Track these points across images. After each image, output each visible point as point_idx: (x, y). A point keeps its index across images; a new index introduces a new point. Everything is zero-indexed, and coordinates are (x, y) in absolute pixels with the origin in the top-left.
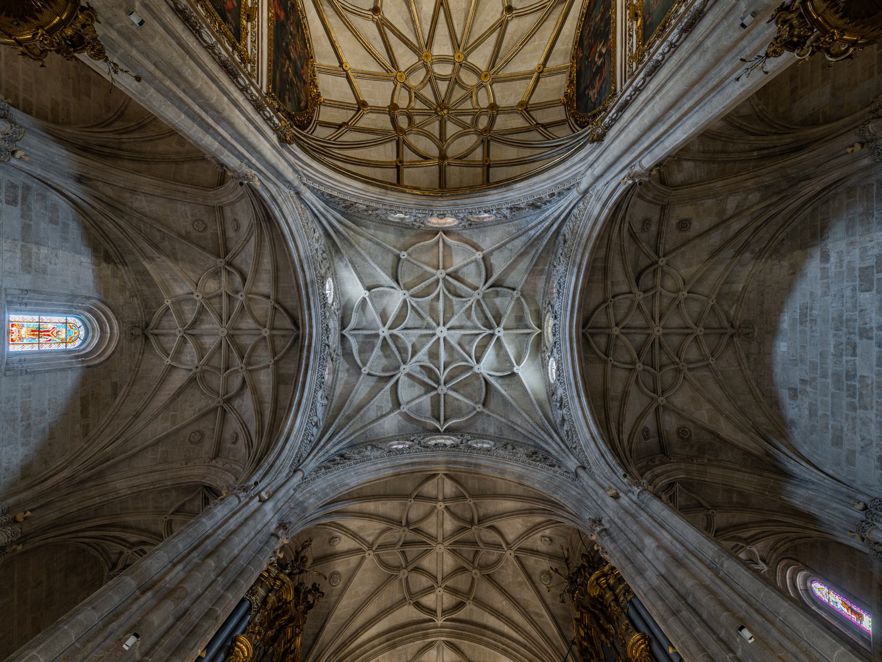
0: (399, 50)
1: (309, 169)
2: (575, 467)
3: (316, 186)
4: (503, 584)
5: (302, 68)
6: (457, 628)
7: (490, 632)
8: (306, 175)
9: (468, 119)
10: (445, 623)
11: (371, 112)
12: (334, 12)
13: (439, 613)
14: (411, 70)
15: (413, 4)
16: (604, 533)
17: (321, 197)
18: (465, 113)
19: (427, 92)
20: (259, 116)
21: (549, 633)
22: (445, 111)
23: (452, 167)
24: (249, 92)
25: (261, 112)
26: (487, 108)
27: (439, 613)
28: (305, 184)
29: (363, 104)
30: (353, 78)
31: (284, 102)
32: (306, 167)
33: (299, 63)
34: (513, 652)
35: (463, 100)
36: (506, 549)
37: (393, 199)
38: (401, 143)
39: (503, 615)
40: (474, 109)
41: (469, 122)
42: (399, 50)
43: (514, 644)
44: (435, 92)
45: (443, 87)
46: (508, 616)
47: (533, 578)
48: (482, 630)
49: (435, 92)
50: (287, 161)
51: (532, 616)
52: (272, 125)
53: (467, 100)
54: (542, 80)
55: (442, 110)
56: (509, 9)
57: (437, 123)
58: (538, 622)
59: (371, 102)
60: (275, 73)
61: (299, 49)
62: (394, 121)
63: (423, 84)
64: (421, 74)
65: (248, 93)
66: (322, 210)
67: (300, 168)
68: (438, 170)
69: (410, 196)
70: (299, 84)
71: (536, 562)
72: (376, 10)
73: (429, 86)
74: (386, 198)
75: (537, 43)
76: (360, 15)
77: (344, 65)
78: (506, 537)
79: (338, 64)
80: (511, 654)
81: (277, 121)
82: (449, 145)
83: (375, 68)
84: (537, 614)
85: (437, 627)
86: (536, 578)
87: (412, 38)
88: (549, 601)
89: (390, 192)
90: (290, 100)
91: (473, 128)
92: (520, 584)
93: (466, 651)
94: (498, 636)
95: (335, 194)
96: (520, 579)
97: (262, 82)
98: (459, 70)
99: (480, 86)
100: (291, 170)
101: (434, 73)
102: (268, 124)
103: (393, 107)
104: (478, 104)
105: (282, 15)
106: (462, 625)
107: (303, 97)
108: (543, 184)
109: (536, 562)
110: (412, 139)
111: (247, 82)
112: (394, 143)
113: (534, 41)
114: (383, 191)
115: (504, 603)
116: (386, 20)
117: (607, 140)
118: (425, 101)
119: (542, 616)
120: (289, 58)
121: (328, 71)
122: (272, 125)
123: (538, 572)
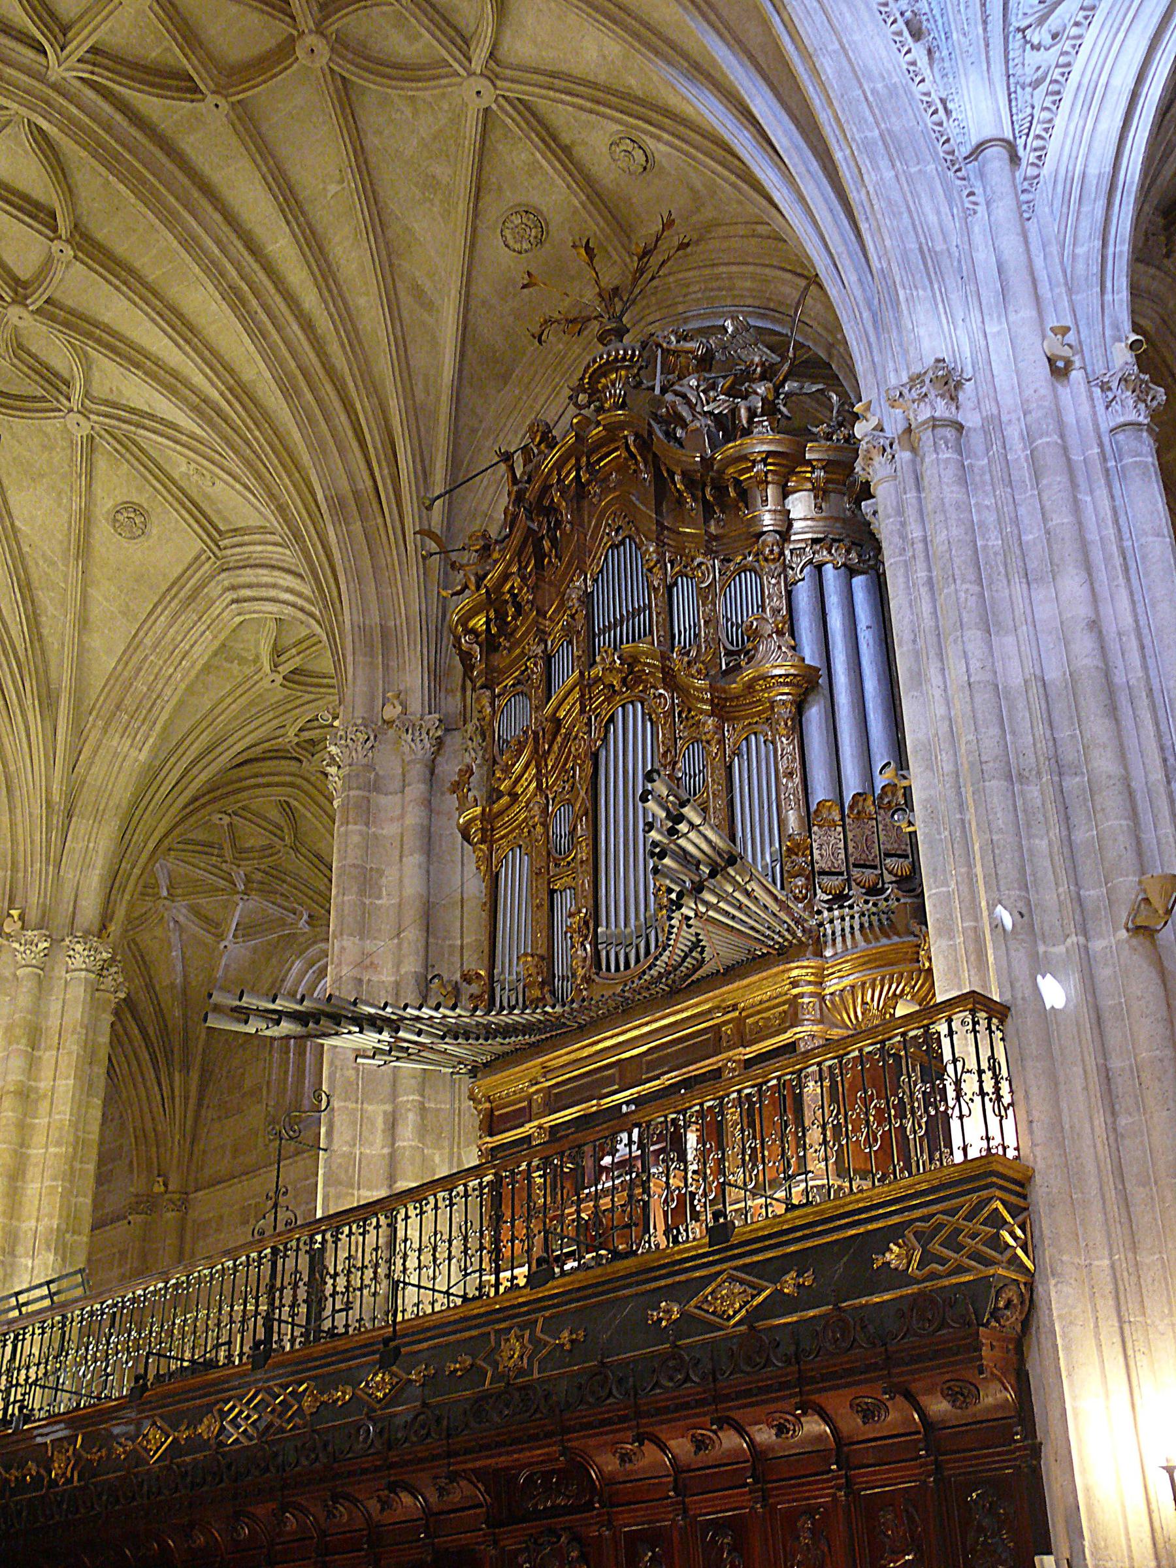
2: (989, 132)
4: (372, 141)
6: (108, 129)
7: (218, 217)
10: (77, 83)
13: (79, 46)
16: (950, 433)
21: (420, 359)
27: (79, 46)
34: (263, 317)
36: (477, 66)
39: (303, 213)
43: (278, 299)
46: (319, 229)
47: (487, 199)
48: (196, 194)
51: (399, 284)
58: (405, 314)
71: (533, 169)
78: (508, 34)
80: (253, 316)
84: (418, 292)
85: (41, 78)
86: (493, 209)
88: (482, 288)
92: (430, 184)
93: (83, 193)
94: (239, 245)
96: (441, 171)
106: (133, 131)
109: (533, 169)
115: (333, 188)
119: (429, 306)
123: (511, 198)
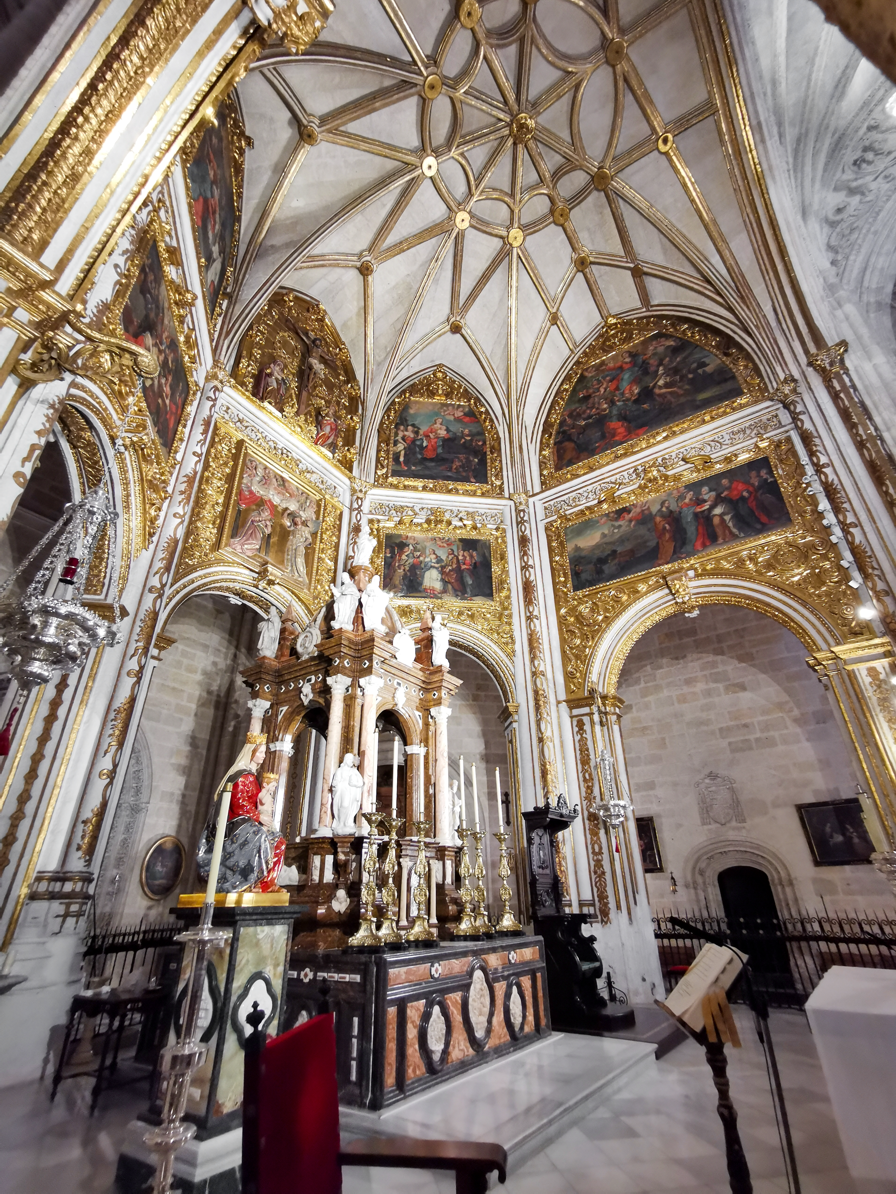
0: (473, 267)
42: (473, 267)
121: (565, 332)
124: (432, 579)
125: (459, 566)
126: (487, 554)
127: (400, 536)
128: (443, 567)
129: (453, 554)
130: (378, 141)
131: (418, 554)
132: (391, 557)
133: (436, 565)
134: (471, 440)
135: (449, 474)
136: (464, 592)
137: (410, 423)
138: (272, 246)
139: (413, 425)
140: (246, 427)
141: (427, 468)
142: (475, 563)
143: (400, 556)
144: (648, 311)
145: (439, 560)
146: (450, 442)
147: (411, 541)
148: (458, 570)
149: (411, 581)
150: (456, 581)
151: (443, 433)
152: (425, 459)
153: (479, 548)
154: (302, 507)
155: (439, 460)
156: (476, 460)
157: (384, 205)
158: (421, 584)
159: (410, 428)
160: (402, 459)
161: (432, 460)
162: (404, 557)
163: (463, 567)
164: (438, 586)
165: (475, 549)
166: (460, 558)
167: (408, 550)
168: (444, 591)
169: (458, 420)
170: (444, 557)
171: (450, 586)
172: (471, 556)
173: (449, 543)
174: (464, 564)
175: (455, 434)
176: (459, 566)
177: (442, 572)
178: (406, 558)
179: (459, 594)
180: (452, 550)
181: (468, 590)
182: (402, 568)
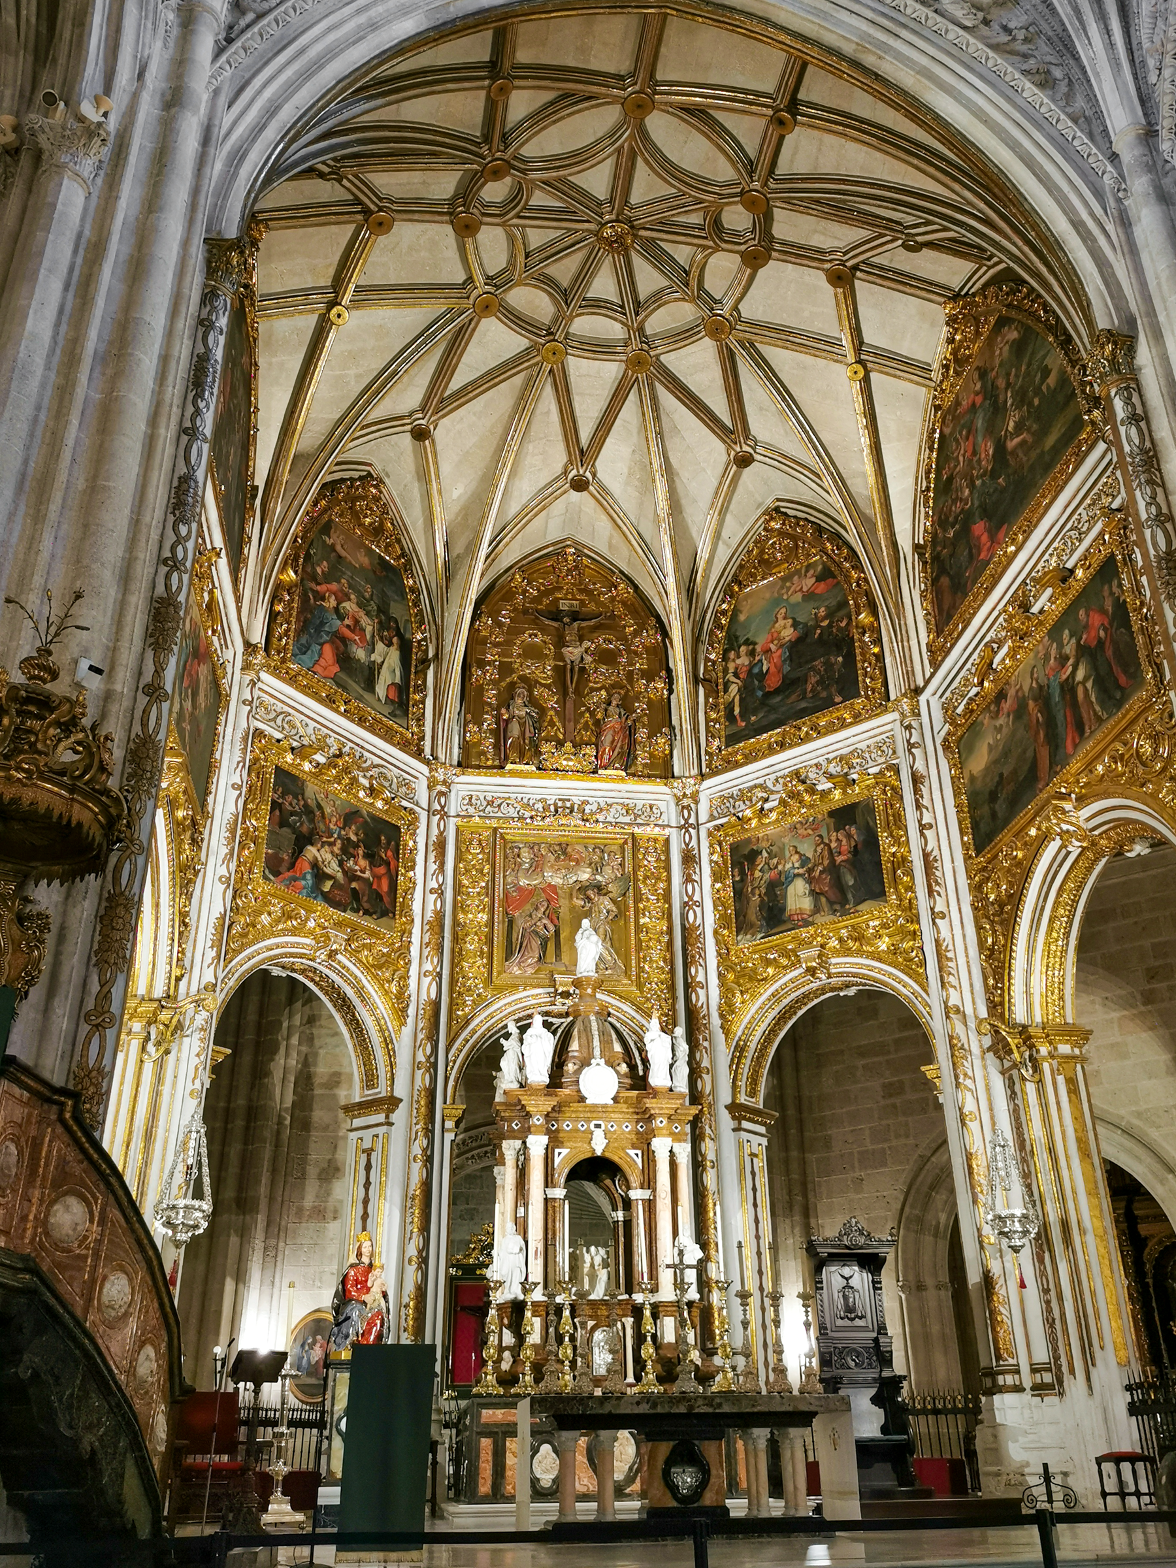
1: (1085, 216)
3: (1082, 142)
5: (973, 407)
8: (1099, 194)
9: (539, 199)
11: (823, 252)
12: (849, 482)
14: (683, 336)
15: (656, 466)
17: (1076, 73)
18: (547, 215)
19: (648, 279)
20: (1157, 436)
22: (608, 232)
23: (612, 70)
24: (1153, 509)
25: (1148, 444)
26: (482, 223)
28: (1114, 157)
29: (839, 278)
30: (846, 341)
31: (1064, 380)
32: (1091, 224)
33: (980, 423)
35: (553, 252)
37: (844, 16)
38: (762, 169)
40: (524, 227)
41: (537, 193)
44: (628, 278)
45: (604, 285)
49: (628, 278)
50: (1138, 269)
52: (1135, 399)
53: (541, 249)
54: (326, 280)
55: (620, 238)
56: (420, 435)
57: (634, 199)
59: (817, 279)
60: (1058, 450)
61: (965, 447)
62: (765, 220)
63: (657, 299)
64: (658, 322)
65: (1159, 507)
66: (1094, 29)
67: (1110, 228)
68: (660, 66)
69: (782, 18)
70: (1001, 383)
72: (744, 461)
73: (644, 292)
74: (864, 26)
75: (352, 372)
76: (786, 457)
77: (861, 374)
79: (873, 375)
81: (1118, 404)
82: (613, 134)
83: (778, 356)
87: (667, 399)
89: (848, 49)
90: (1046, 372)
91: (532, 181)
95: (1029, 89)
97: (1103, 457)
98: (555, 320)
99: (500, 281)
100: (1138, 232)
101: (622, 322)
102: (1143, 404)
103: (754, 260)
104: (511, 239)
105: (979, 528)
107: (1002, 350)
108: (332, 37)
110: (723, 171)
111: (1148, 533)
112: (782, 168)
113: (359, 376)
114: (869, 60)
116: (724, 442)
117: (198, 252)
118: (660, 259)
120: (1000, 448)
122: (1135, 399)
124: (798, 897)
125: (833, 861)
126: (871, 823)
127: (748, 840)
128: (810, 871)
129: (822, 842)
130: (482, 377)
131: (775, 861)
132: (742, 880)
133: (801, 871)
134: (830, 626)
135: (803, 705)
136: (844, 902)
137: (742, 640)
138: (458, 556)
139: (747, 642)
140: (499, 806)
141: (773, 709)
142: (856, 846)
143: (752, 875)
144: (990, 268)
145: (804, 861)
146: (799, 649)
147: (764, 844)
148: (833, 869)
149: (770, 909)
150: (831, 887)
151: (788, 634)
152: (768, 695)
153: (859, 818)
154: (597, 868)
155: (790, 684)
156: (840, 659)
157: (548, 412)
158: (783, 909)
159: (743, 649)
160: (737, 711)
161: (777, 691)
162: (757, 874)
163: (839, 859)
164: (807, 904)
165: (853, 822)
166: (833, 845)
167: (761, 861)
168: (817, 910)
169: (809, 596)
170: (810, 855)
171: (823, 899)
172: (849, 836)
173: (814, 825)
174: (840, 853)
175: (806, 625)
176: (833, 861)
177: (810, 881)
178: (760, 876)
179: (837, 907)
180: (821, 836)
181: (850, 896)
182: (757, 892)
